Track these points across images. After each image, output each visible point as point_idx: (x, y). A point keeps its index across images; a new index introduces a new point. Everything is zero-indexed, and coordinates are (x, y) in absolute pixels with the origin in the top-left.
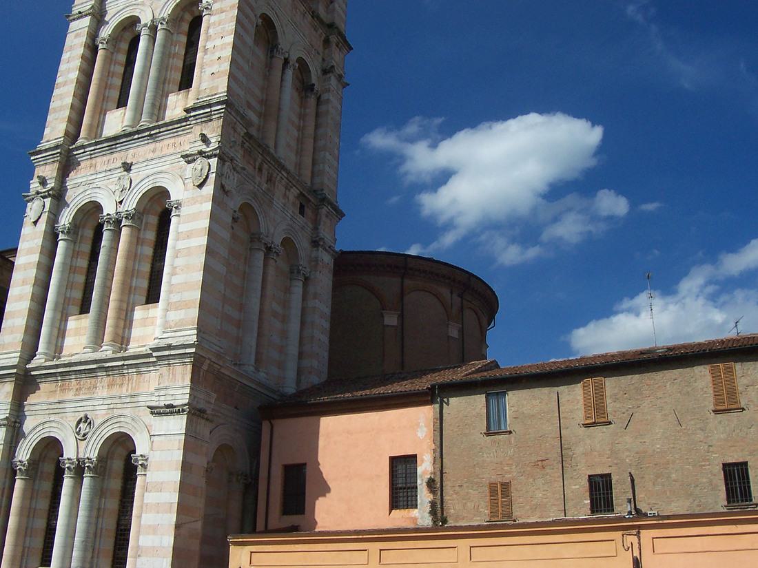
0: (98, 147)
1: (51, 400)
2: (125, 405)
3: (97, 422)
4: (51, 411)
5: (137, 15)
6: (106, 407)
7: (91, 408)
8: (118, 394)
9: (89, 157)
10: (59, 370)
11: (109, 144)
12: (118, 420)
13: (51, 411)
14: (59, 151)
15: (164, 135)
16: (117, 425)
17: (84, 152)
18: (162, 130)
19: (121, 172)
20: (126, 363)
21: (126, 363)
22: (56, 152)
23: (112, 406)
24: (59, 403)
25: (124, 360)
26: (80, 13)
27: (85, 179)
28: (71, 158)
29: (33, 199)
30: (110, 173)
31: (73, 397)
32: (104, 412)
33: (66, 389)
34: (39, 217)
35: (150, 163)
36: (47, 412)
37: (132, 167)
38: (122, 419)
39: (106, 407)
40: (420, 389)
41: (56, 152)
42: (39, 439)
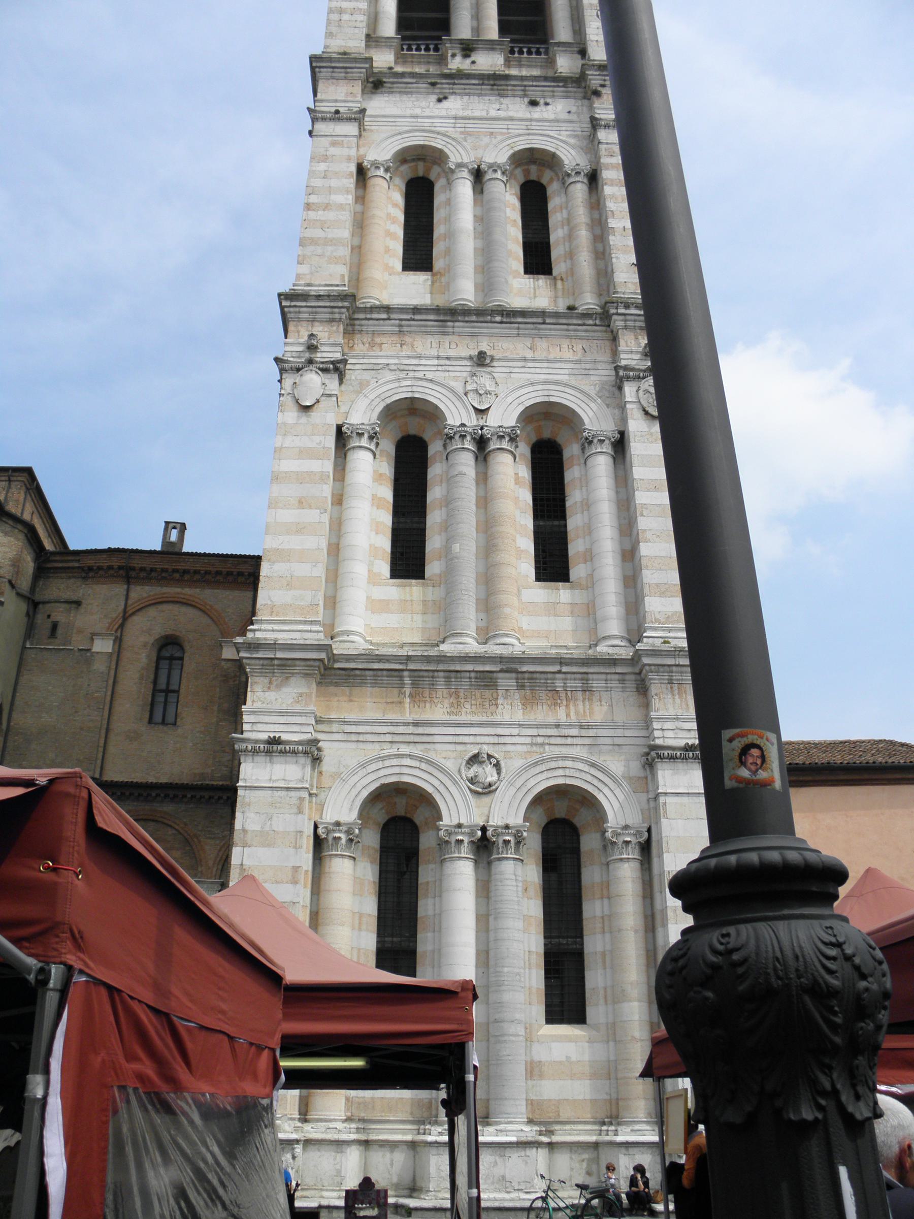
0: (418, 317)
1: (391, 716)
2: (569, 741)
3: (510, 766)
4: (397, 738)
5: (440, 147)
6: (528, 740)
7: (495, 740)
8: (551, 719)
9: (397, 329)
10: (412, 666)
11: (442, 318)
12: (561, 763)
13: (397, 738)
14: (346, 304)
15: (550, 330)
16: (560, 772)
17: (389, 319)
18: (548, 321)
19: (463, 370)
20: (565, 669)
21: (565, 669)
22: (340, 304)
23: (540, 740)
24: (416, 724)
25: (561, 664)
26: (337, 112)
27: (396, 361)
28: (357, 322)
29: (302, 368)
30: (448, 362)
31: (446, 718)
32: (525, 748)
33: (425, 702)
34: (318, 401)
35: (530, 365)
36: (389, 738)
37: (495, 364)
38: (569, 764)
39: (528, 740)
40: (901, 761)
41: (340, 304)
42: (377, 785)
